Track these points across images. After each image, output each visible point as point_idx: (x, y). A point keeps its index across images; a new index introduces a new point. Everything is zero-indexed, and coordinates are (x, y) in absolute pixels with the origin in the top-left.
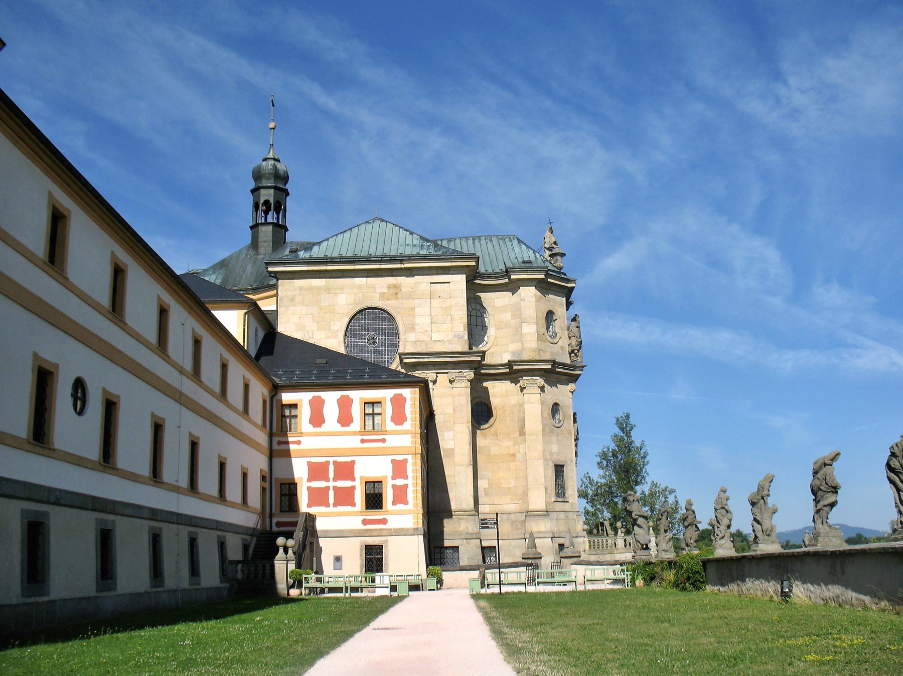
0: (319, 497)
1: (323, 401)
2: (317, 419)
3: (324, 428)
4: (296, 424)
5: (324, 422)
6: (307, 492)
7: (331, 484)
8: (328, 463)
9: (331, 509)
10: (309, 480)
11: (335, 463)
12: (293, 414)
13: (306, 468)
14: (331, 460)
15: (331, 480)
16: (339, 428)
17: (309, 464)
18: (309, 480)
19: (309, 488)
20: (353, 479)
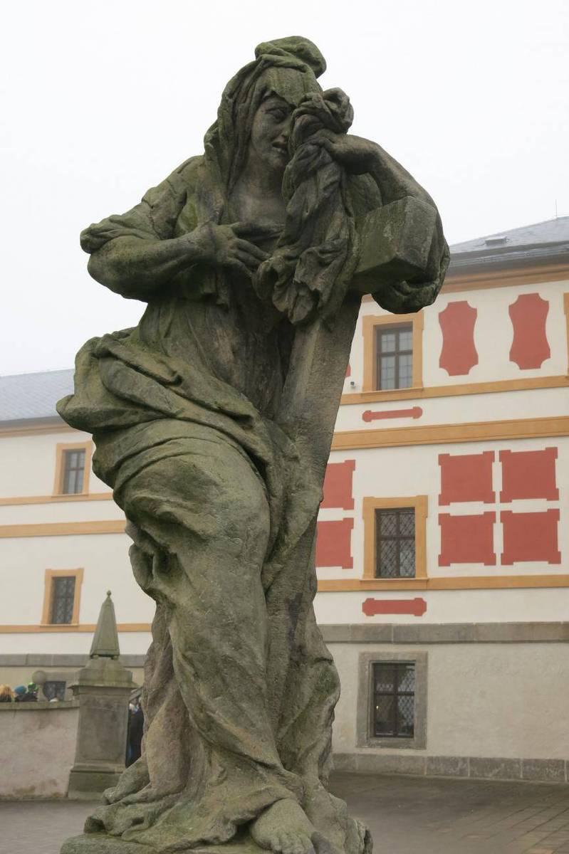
0: (465, 541)
1: (473, 314)
2: (459, 355)
3: (477, 375)
4: (409, 366)
5: (472, 359)
6: (439, 528)
7: (498, 507)
8: (489, 456)
9: (499, 570)
10: (444, 500)
11: (505, 455)
12: (403, 347)
13: (438, 469)
14: (497, 448)
15: (498, 497)
16: (514, 372)
17: (443, 459)
18: (444, 500)
19: (444, 519)
20: (553, 494)
